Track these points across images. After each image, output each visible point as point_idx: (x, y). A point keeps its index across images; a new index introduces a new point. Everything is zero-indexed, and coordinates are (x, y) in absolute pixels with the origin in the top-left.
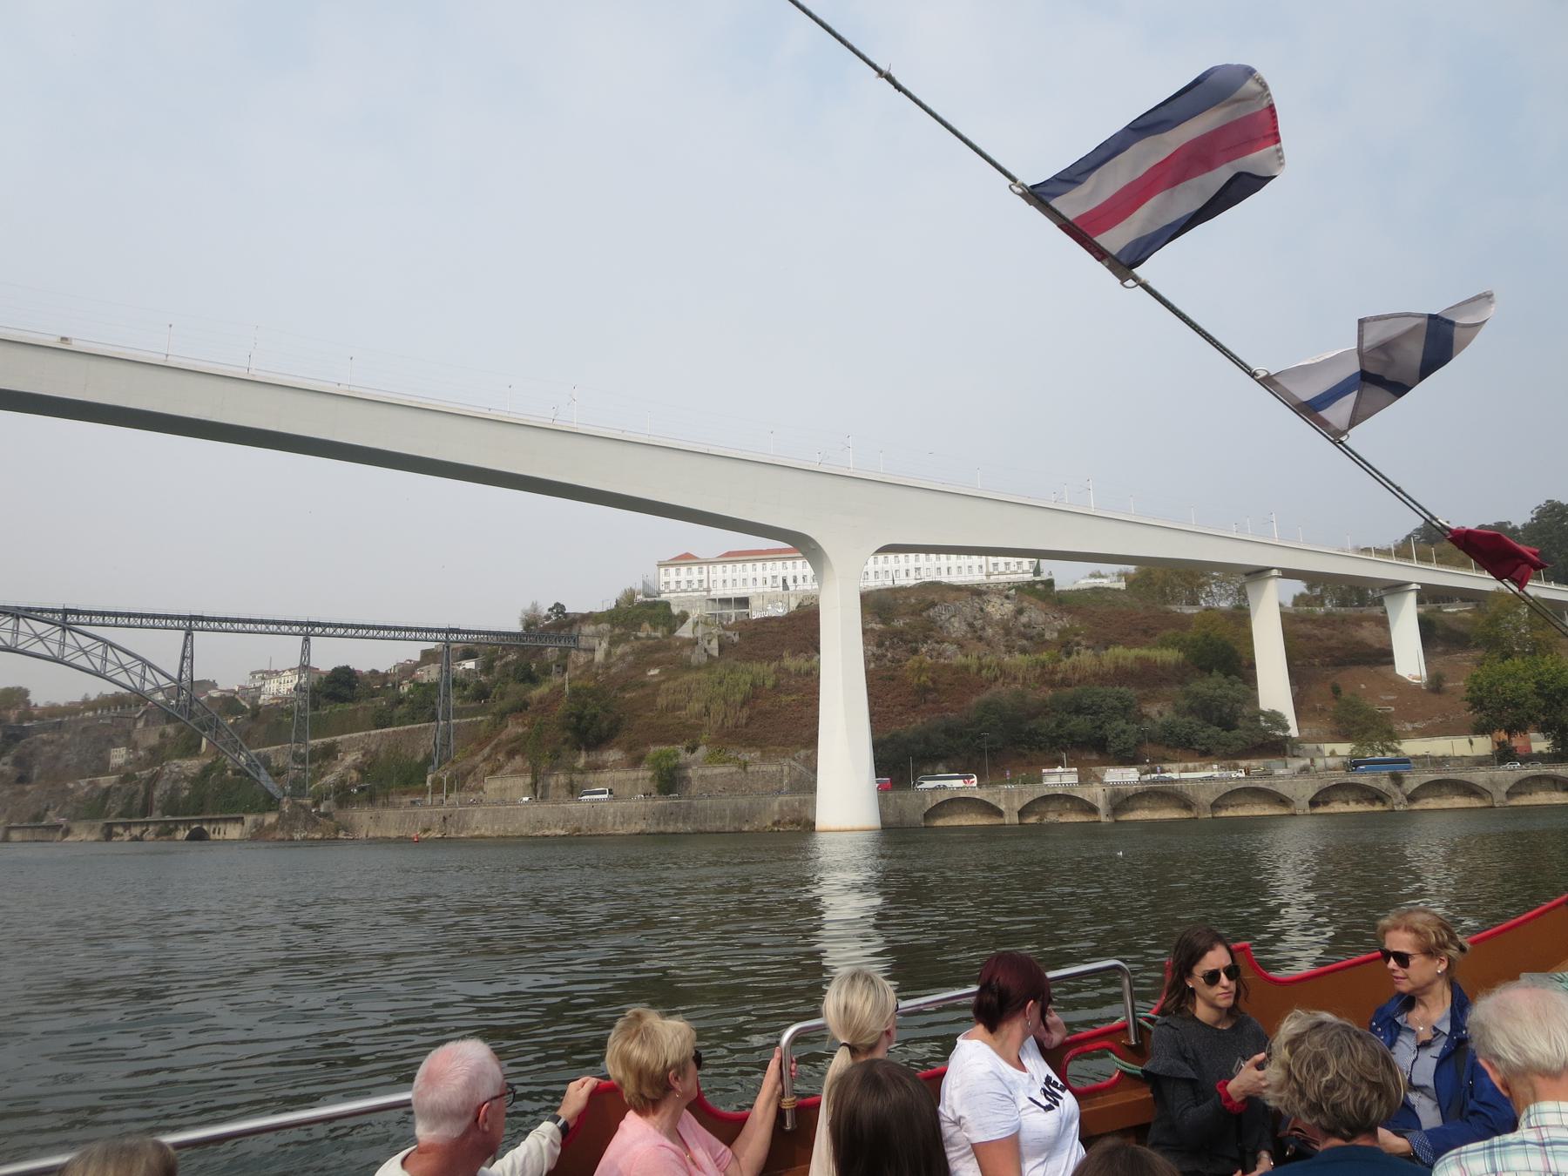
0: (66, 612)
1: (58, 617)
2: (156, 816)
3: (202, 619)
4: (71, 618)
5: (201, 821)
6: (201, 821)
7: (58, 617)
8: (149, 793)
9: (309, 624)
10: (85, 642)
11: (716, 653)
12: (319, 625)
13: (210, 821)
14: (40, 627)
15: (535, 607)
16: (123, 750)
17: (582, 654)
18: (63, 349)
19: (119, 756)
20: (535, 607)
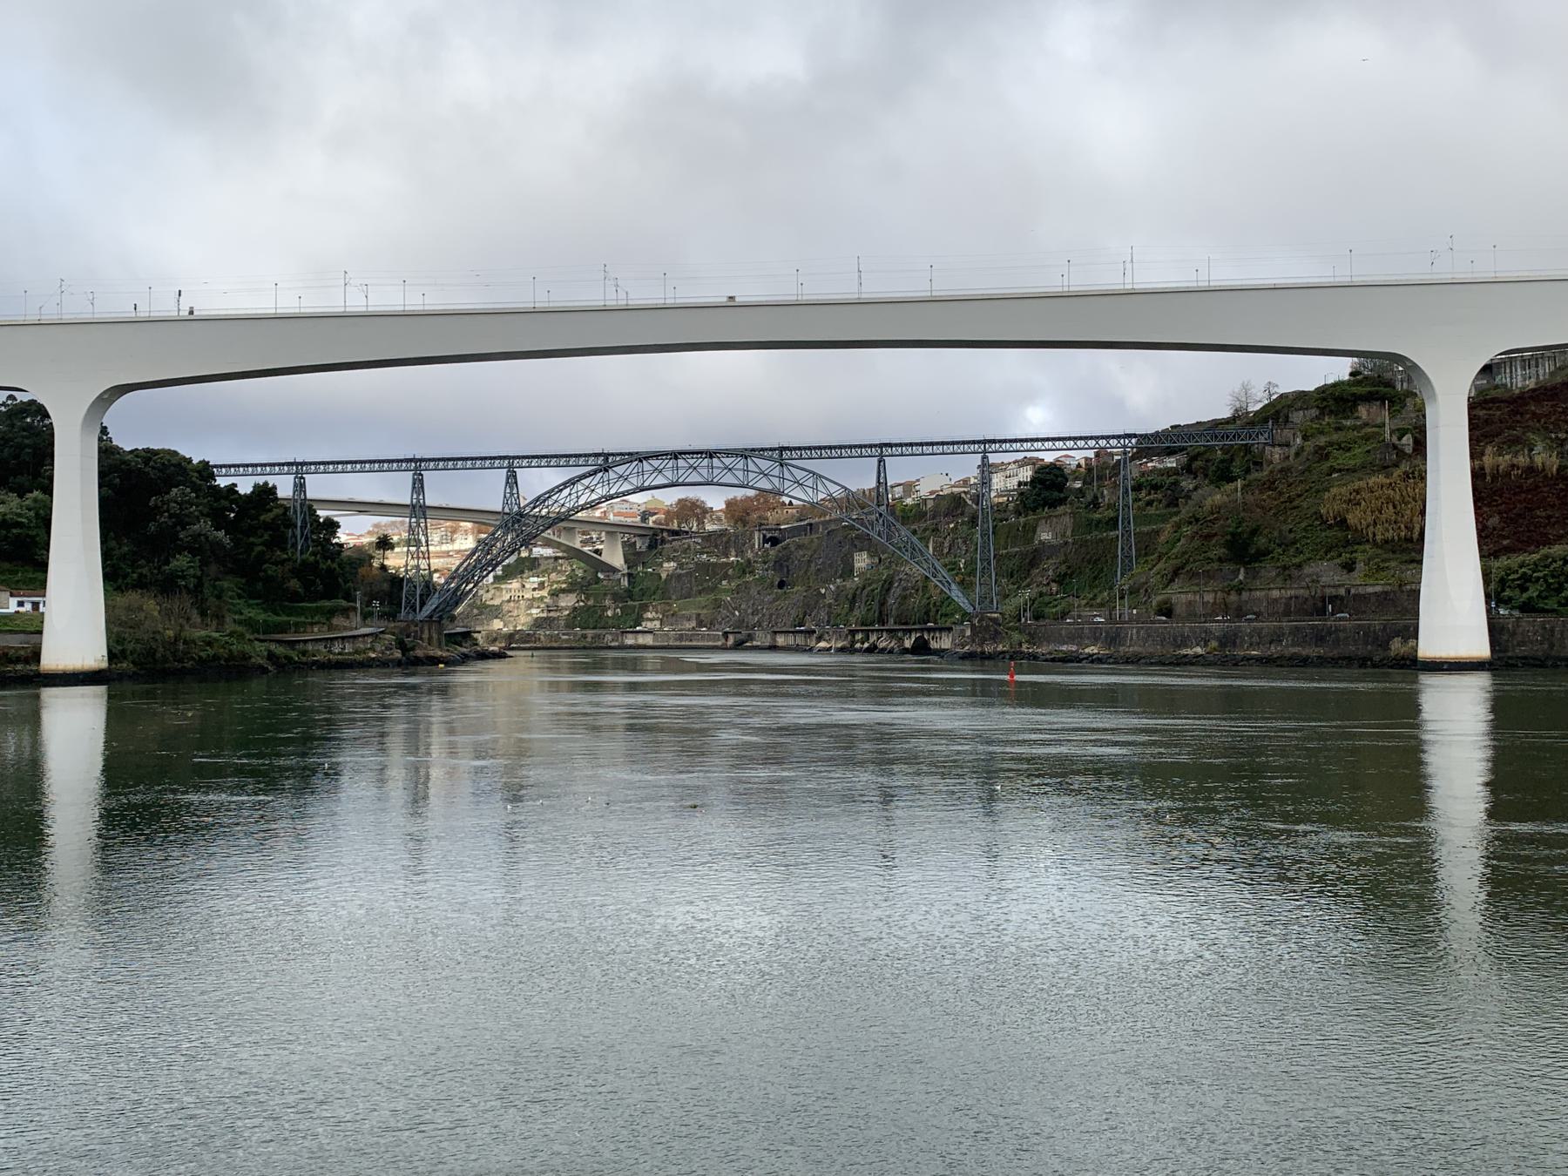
0: (782, 449)
1: (776, 454)
2: (891, 625)
3: (890, 445)
4: (786, 455)
5: (922, 630)
6: (922, 630)
7: (776, 454)
8: (883, 604)
9: (984, 442)
10: (799, 474)
11: (1409, 450)
12: (994, 441)
13: (929, 630)
14: (764, 464)
15: (1246, 389)
16: (865, 555)
17: (1277, 449)
18: (731, 304)
19: (862, 561)
20: (1246, 389)
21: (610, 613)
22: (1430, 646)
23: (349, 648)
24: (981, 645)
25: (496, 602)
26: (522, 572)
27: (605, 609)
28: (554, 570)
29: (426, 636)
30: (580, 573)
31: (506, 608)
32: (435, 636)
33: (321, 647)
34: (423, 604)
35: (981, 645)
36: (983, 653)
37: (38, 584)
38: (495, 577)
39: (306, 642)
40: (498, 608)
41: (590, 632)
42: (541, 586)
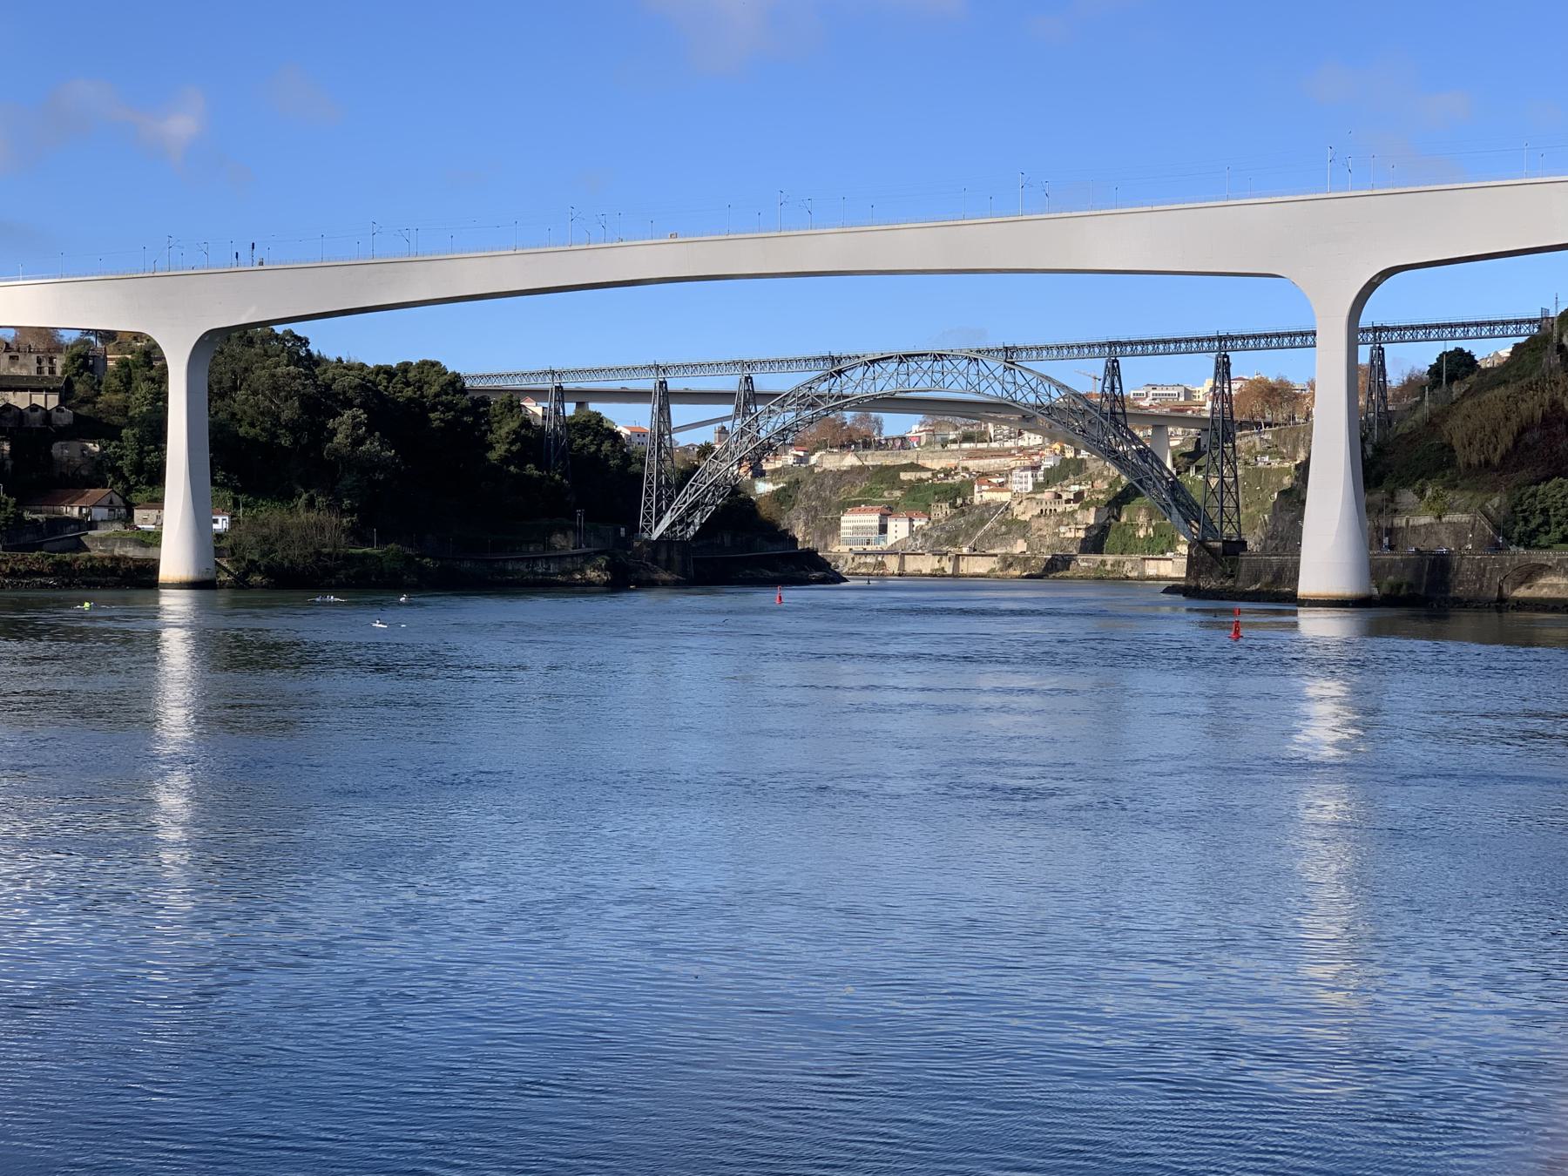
14: (992, 365)
21: (1142, 533)
22: (1308, 585)
23: (553, 568)
24: (1196, 579)
25: (1026, 517)
26: (1066, 478)
27: (1138, 527)
28: (1100, 475)
29: (663, 556)
30: (1124, 479)
31: (1035, 525)
32: (677, 558)
33: (523, 567)
34: (657, 524)
35: (1196, 579)
36: (1198, 587)
37: (157, 502)
38: (1036, 485)
39: (506, 561)
40: (1026, 525)
41: (1110, 559)
42: (1078, 496)
